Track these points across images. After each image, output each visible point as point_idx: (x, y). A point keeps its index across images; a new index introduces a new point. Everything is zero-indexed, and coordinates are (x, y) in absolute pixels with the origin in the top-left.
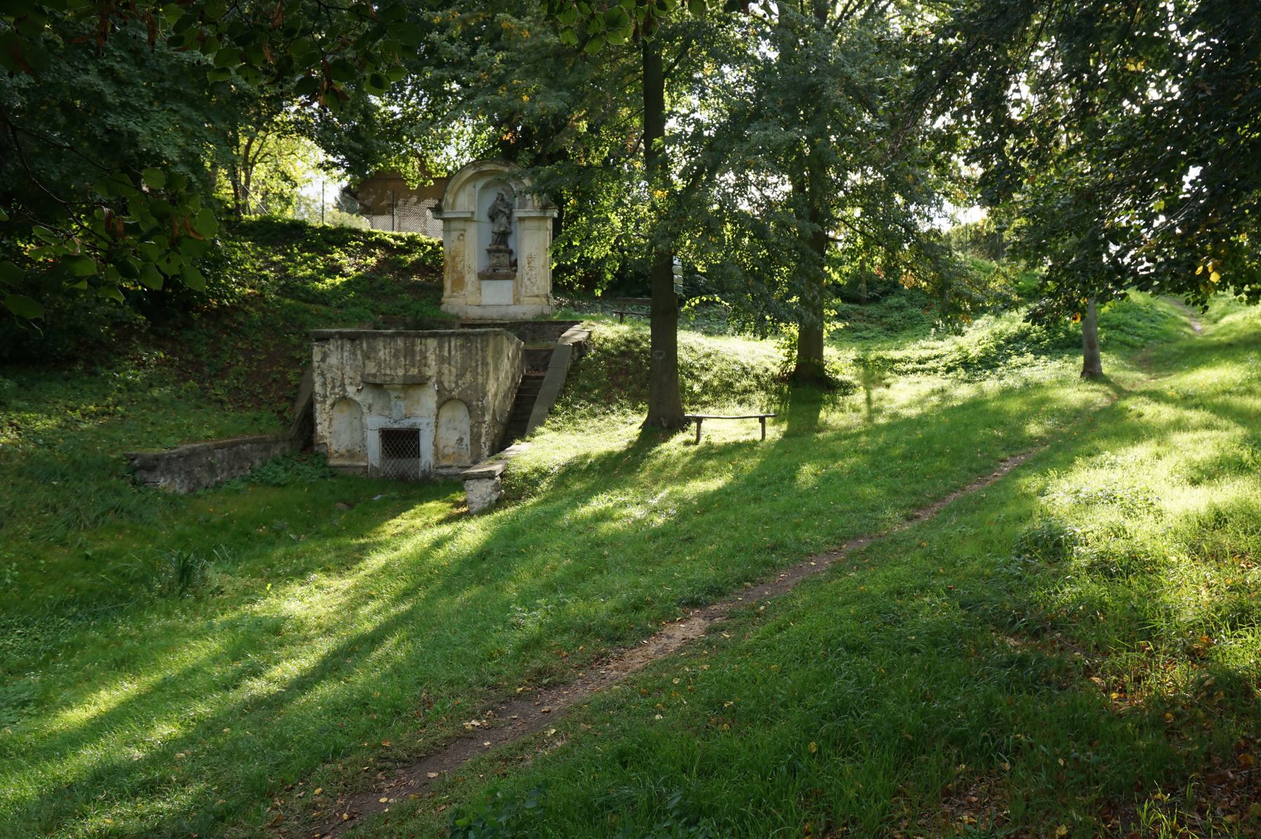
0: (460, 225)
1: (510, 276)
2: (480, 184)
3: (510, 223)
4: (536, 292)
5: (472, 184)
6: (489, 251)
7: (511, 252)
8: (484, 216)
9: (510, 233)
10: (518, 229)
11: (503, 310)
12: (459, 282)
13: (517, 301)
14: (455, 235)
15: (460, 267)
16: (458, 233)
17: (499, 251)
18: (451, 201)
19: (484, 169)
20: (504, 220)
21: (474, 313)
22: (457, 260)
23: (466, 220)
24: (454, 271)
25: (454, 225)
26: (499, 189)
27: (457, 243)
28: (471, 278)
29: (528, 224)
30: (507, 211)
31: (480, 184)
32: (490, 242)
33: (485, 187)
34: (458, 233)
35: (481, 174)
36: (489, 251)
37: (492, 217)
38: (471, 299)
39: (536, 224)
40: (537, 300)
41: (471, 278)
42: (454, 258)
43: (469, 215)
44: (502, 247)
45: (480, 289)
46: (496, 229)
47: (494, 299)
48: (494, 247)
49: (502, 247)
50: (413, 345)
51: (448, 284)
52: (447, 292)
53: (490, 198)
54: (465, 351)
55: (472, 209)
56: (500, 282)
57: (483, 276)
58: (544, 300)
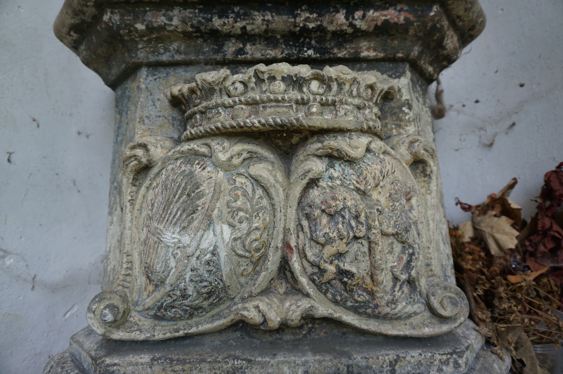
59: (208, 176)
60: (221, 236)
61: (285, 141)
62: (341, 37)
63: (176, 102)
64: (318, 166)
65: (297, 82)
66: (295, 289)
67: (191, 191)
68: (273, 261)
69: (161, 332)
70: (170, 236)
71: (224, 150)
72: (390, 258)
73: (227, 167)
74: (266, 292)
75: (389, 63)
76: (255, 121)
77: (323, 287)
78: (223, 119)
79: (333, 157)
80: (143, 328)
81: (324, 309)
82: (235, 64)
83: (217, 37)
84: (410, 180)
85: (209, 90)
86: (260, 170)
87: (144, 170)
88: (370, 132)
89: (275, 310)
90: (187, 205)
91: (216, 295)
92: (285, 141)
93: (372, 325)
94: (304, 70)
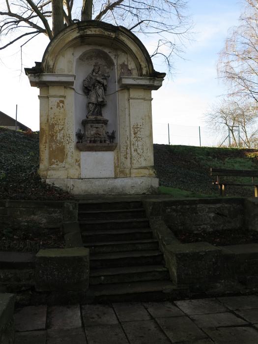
2: (79, 53)
4: (144, 164)
7: (105, 122)
8: (78, 85)
14: (54, 101)
15: (59, 136)
16: (58, 100)
19: (89, 32)
22: (57, 128)
24: (52, 140)
25: (53, 91)
30: (105, 82)
31: (79, 53)
33: (81, 59)
34: (58, 100)
37: (87, 90)
38: (73, 172)
43: (71, 79)
44: (99, 117)
45: (78, 161)
46: (93, 99)
48: (92, 117)
49: (99, 117)
51: (45, 154)
56: (100, 154)
58: (151, 172)
61: (97, 128)
90: (93, 131)
92: (97, 128)
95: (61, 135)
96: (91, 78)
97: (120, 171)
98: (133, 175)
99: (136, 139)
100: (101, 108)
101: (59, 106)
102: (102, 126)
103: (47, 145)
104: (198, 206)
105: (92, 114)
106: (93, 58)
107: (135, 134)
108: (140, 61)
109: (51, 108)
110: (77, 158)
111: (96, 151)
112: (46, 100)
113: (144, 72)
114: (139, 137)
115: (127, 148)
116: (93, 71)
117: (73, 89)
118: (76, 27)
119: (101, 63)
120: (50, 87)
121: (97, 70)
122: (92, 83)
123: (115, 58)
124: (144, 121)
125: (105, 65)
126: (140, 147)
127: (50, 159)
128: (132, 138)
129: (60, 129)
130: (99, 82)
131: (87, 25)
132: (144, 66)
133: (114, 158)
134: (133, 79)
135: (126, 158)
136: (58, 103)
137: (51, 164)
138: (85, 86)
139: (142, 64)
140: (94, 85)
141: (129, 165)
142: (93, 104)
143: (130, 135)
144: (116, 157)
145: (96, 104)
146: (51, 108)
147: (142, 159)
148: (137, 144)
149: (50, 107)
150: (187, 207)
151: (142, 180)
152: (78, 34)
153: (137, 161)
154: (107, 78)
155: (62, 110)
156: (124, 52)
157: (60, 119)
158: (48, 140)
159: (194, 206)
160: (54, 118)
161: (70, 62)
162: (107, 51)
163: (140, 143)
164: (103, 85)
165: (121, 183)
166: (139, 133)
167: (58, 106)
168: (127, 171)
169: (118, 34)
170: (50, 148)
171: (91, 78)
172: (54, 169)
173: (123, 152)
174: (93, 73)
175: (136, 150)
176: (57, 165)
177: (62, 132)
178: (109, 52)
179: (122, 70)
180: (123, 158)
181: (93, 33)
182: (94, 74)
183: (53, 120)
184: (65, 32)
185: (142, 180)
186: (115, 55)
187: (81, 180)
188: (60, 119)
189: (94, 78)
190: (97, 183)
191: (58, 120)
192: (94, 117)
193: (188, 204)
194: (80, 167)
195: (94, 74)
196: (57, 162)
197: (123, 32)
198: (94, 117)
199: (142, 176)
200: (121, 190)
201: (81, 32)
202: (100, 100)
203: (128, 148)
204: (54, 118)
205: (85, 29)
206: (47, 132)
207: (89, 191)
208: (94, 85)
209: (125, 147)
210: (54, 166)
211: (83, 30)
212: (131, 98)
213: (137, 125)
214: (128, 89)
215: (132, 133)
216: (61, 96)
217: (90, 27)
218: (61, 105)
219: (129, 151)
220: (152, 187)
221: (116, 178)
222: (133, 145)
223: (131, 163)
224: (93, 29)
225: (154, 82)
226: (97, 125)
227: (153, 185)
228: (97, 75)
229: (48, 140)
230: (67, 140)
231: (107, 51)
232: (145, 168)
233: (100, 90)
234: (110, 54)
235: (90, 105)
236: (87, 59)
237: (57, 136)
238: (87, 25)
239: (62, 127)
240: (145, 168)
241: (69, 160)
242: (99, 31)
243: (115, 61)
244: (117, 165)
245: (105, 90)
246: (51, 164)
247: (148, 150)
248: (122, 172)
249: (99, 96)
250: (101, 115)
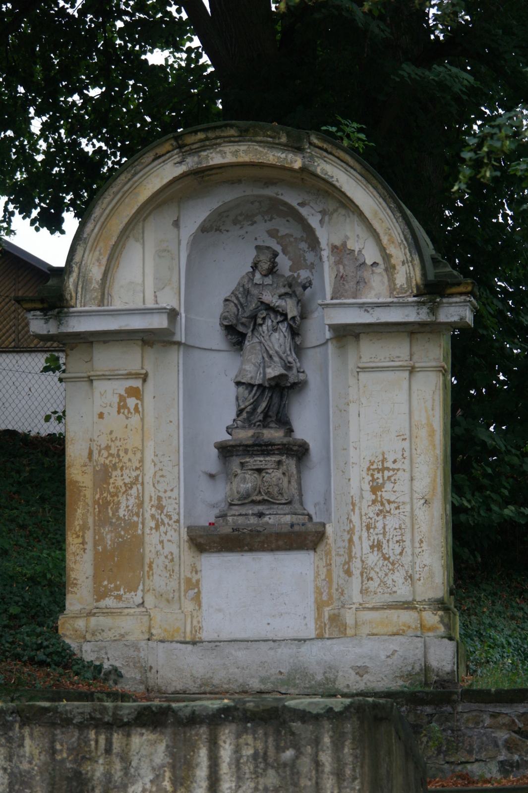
0: (130, 359)
1: (305, 538)
3: (299, 350)
4: (403, 592)
5: (166, 218)
6: (226, 451)
9: (299, 386)
10: (322, 367)
11: (282, 659)
12: (123, 561)
13: (333, 625)
14: (108, 392)
15: (125, 505)
16: (121, 386)
17: (263, 448)
18: (96, 273)
19: (215, 158)
20: (278, 340)
21: (177, 669)
22: (118, 479)
23: (148, 339)
24: (103, 520)
26: (260, 233)
27: (115, 421)
28: (164, 544)
29: (371, 351)
30: (291, 308)
31: (196, 215)
32: (229, 415)
35: (201, 180)
36: (226, 451)
37: (236, 335)
38: (164, 619)
39: (397, 351)
40: (407, 617)
41: (164, 544)
42: (103, 475)
43: (159, 322)
44: (274, 434)
45: (193, 586)
46: (252, 373)
47: (251, 616)
48: (245, 435)
49: (274, 434)
50: (82, 755)
51: (81, 566)
52: (78, 599)
53: (232, 266)
54: (271, 779)
55: (168, 300)
56: (266, 560)
57: (207, 541)
58: (432, 618)
59: (247, 476)
60: (250, 485)
61: (259, 471)
62: (271, 450)
63: (241, 463)
64: (264, 474)
65: (261, 461)
66: (262, 495)
67: (245, 478)
68: (257, 490)
69: (240, 502)
70: (242, 485)
71: (250, 472)
72: (276, 489)
73: (250, 475)
74: (257, 495)
75: (281, 454)
76: (254, 468)
77: (266, 494)
78: (250, 467)
79: (267, 473)
80: (236, 502)
81: (266, 498)
82: (252, 455)
83: (249, 451)
84: (282, 476)
85: (247, 462)
86: (255, 475)
87: (236, 476)
88: (273, 469)
89: (259, 498)
90: (244, 480)
91: (248, 495)
92: (259, 471)
93: (275, 501)
94: (262, 459)
95: (132, 501)
96: (247, 293)
97: (330, 618)
98: (365, 630)
99: (378, 507)
100: (281, 397)
101: (125, 406)
102: (279, 463)
103: (89, 536)
104: (460, 709)
105: (249, 422)
106: (259, 218)
107: (375, 489)
108: (385, 240)
109: (101, 416)
110: (189, 575)
111: (251, 550)
112: (85, 385)
113: (400, 279)
114: (389, 502)
115: (351, 541)
116: (255, 266)
117: (179, 344)
118: (170, 148)
119: (287, 231)
120: (95, 346)
121: (265, 266)
122: (247, 314)
123: (321, 222)
124: (406, 444)
125: (302, 240)
126: (390, 533)
127: (97, 578)
128: (365, 504)
129: (127, 480)
130: (269, 308)
131: (207, 139)
132: (402, 258)
133: (317, 575)
134: (361, 306)
135: (349, 573)
136: (121, 396)
137: (100, 595)
138: (226, 323)
139: (392, 250)
140: (254, 317)
141: (357, 598)
142: (250, 386)
143: (362, 497)
144: (323, 572)
145: (260, 386)
146: (101, 416)
147: (399, 576)
148: (380, 525)
149: (98, 410)
150: (429, 709)
151: (394, 644)
152: (182, 169)
153: (383, 583)
154: (299, 290)
155: (135, 419)
156: (343, 205)
157: (126, 451)
158: (90, 521)
159: (448, 709)
160: (108, 448)
161: (161, 253)
162: (292, 199)
163: (392, 522)
164: (285, 315)
165: (315, 656)
166: (388, 486)
167: (122, 406)
168: (349, 617)
169: (312, 157)
170: (96, 544)
171: (247, 293)
172: (108, 612)
173: (342, 551)
174: (253, 273)
175: (377, 546)
176: (119, 598)
177: (134, 491)
178: (302, 204)
179: (341, 267)
180: (342, 574)
181: (229, 159)
182: (258, 276)
183: (105, 454)
184: (139, 168)
185: (392, 647)
186: (323, 213)
187: (190, 647)
188: (126, 451)
189: (255, 291)
190: (241, 654)
191: (122, 454)
192: (250, 433)
193: (428, 703)
194: (200, 605)
195: (258, 276)
196: (117, 588)
197: (326, 151)
198: (250, 433)
199: (391, 635)
200: (319, 677)
201: (191, 163)
202: (273, 371)
203: (356, 538)
204: (108, 448)
205: (204, 148)
206: (88, 493)
207: (216, 681)
208: (254, 317)
209: (346, 537)
210: (109, 602)
211: (196, 152)
212: (364, 369)
213: (384, 460)
214: (357, 337)
215: (366, 487)
216: (130, 376)
217: (218, 141)
218: (132, 402)
219: (356, 550)
220: (427, 669)
221: (320, 637)
222: (368, 527)
223: (364, 591)
224: (229, 149)
225: (433, 311)
226: (259, 461)
227: (434, 663)
228: (268, 280)
229: (90, 521)
230: (153, 516)
231: (292, 199)
232: (407, 606)
233: (276, 335)
234: (304, 211)
235: (241, 389)
236: (235, 222)
237: (119, 503)
238: (207, 139)
239: (134, 474)
240: (407, 606)
241: (159, 581)
242: (245, 152)
243: (322, 234)
244: (325, 597)
245: (294, 332)
246: (100, 595)
247: (425, 546)
248: (335, 619)
249: (271, 357)
250: (285, 424)
